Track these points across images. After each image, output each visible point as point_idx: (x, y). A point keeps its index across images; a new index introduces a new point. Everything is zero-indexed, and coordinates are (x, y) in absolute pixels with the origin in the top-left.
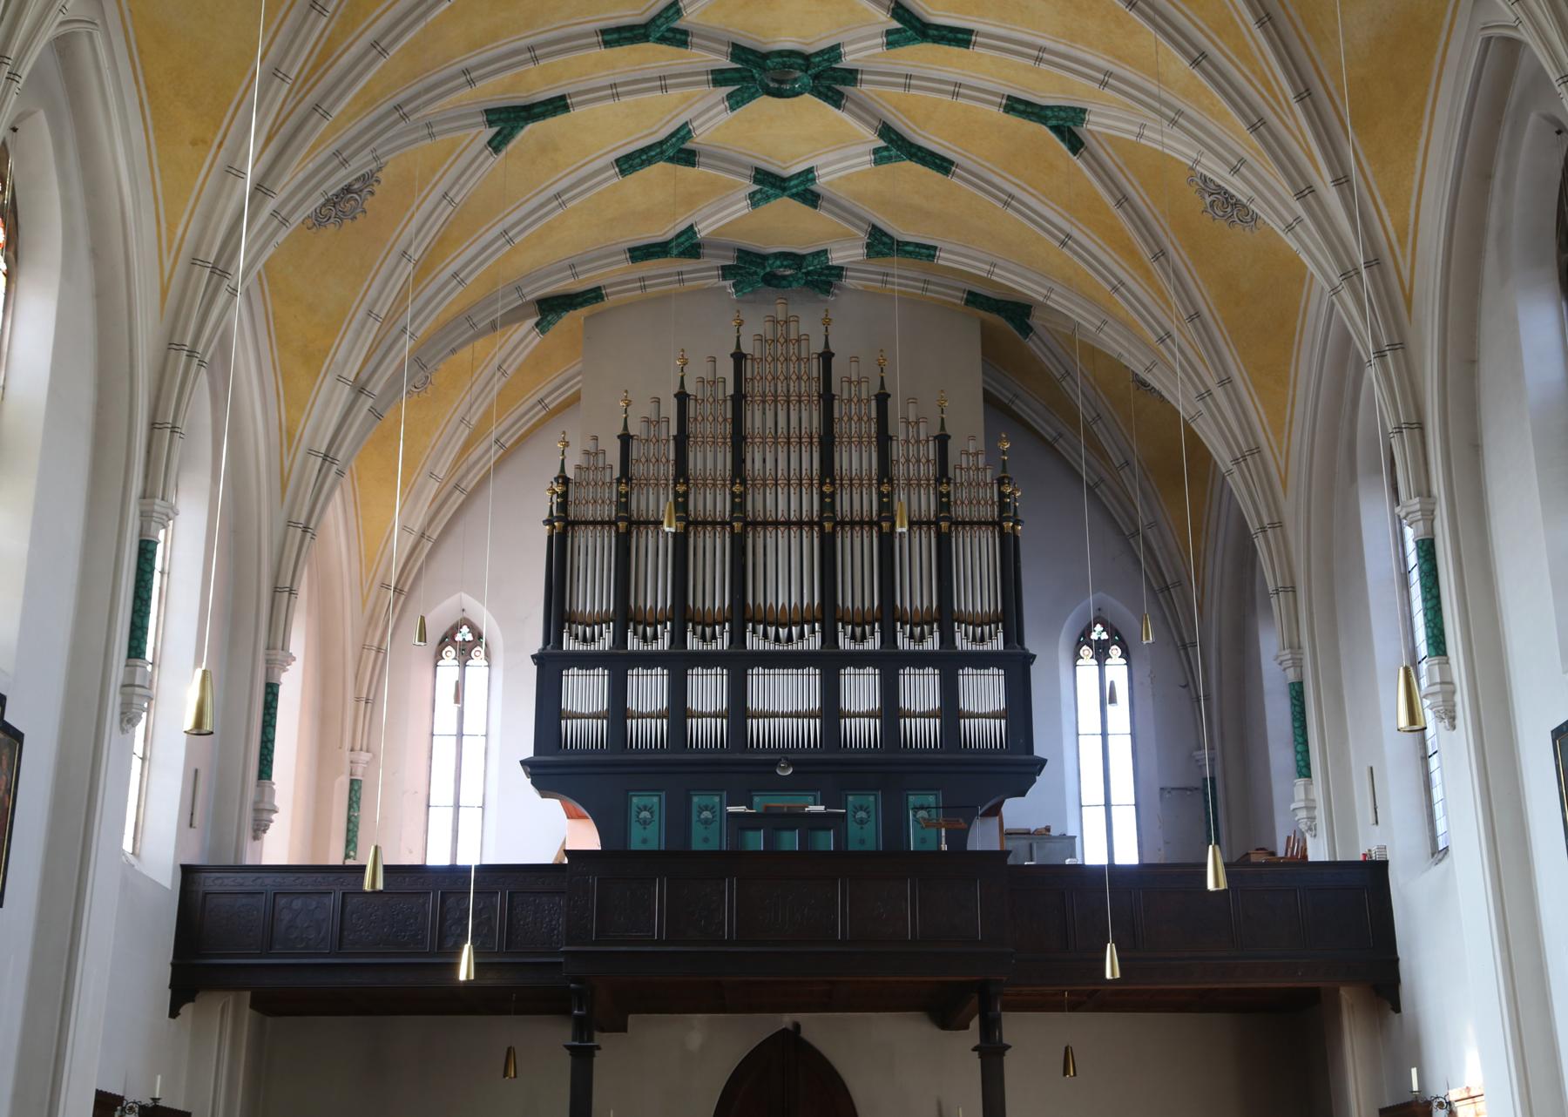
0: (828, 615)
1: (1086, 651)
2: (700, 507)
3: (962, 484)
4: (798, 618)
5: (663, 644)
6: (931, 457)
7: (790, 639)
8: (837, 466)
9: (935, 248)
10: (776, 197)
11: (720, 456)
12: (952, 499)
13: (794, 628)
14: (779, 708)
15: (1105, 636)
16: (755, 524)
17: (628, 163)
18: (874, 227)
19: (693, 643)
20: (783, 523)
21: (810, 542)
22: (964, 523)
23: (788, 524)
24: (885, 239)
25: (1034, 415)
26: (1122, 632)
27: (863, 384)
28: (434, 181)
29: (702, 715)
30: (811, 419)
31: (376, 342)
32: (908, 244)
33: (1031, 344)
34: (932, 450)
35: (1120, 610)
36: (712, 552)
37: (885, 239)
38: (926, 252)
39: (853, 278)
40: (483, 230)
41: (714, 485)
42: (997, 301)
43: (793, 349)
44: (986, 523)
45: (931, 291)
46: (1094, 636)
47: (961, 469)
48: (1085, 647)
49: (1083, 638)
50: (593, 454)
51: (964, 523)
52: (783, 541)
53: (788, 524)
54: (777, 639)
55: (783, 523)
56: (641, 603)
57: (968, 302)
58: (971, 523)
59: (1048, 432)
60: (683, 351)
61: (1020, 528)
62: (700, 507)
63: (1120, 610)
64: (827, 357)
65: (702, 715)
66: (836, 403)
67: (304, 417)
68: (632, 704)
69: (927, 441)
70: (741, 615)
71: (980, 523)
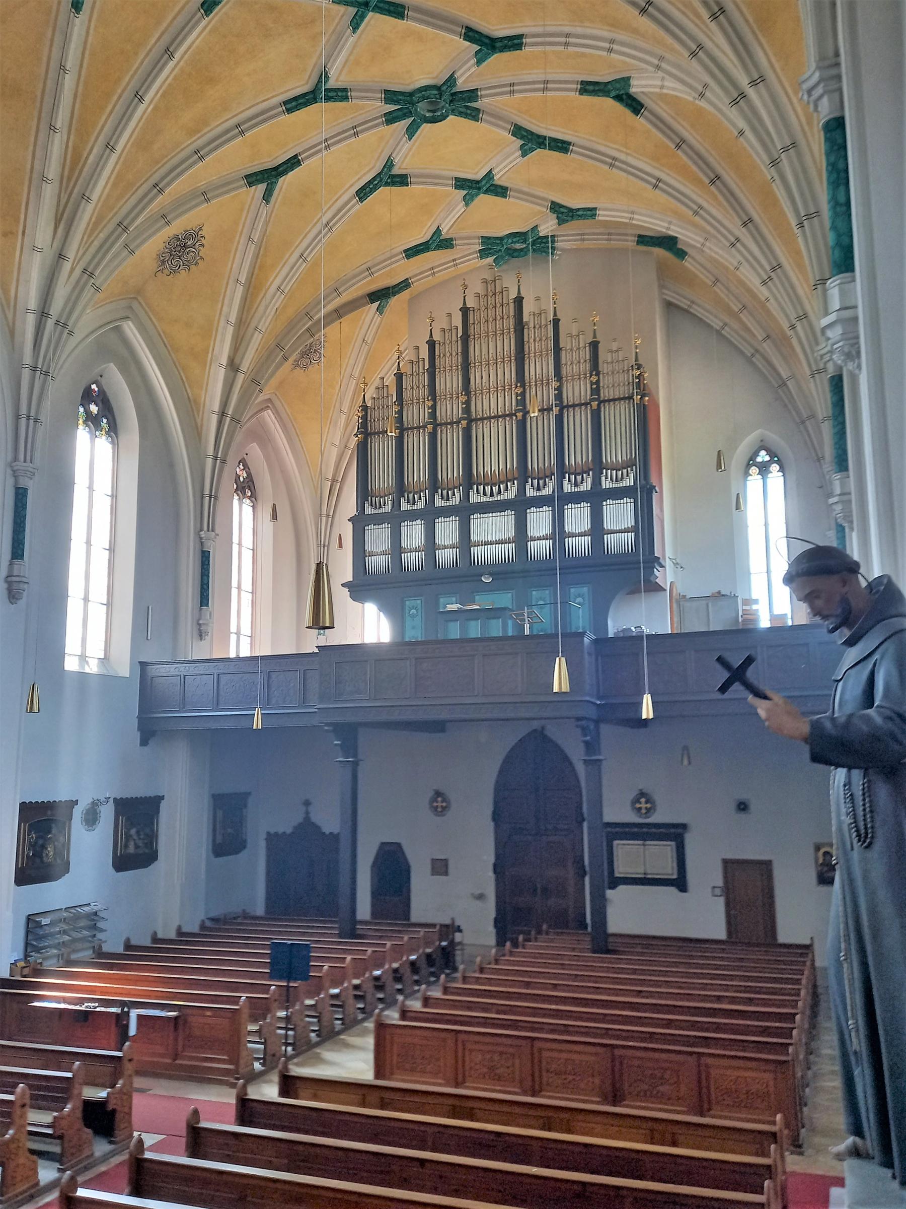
0: (523, 474)
1: (754, 470)
2: (444, 414)
3: (608, 373)
4: (502, 478)
5: (420, 505)
6: (588, 357)
7: (499, 492)
8: (527, 374)
9: (595, 209)
10: (477, 195)
11: (455, 378)
12: (601, 385)
13: (501, 486)
14: (491, 538)
15: (767, 458)
16: (476, 420)
17: (363, 193)
18: (553, 203)
19: (439, 502)
20: (494, 417)
21: (511, 426)
22: (609, 401)
23: (497, 417)
24: (562, 210)
25: (707, 314)
26: (780, 456)
27: (543, 315)
28: (240, 230)
29: (445, 547)
30: (508, 345)
31: (239, 339)
32: (579, 210)
33: (686, 264)
34: (586, 354)
35: (774, 438)
36: (451, 440)
37: (562, 210)
38: (590, 213)
39: (562, 241)
40: (288, 255)
41: (452, 398)
42: (658, 238)
43: (498, 298)
44: (624, 398)
45: (614, 240)
46: (759, 459)
47: (607, 363)
48: (754, 468)
49: (751, 461)
50: (382, 388)
51: (609, 401)
52: (494, 429)
53: (497, 417)
54: (492, 495)
55: (494, 417)
56: (410, 479)
57: (638, 243)
58: (614, 400)
59: (716, 324)
60: (431, 312)
61: (647, 398)
62: (444, 414)
63: (774, 438)
64: (519, 301)
65: (445, 547)
66: (526, 331)
67: (204, 392)
68: (404, 544)
69: (585, 347)
70: (469, 481)
71: (620, 399)
